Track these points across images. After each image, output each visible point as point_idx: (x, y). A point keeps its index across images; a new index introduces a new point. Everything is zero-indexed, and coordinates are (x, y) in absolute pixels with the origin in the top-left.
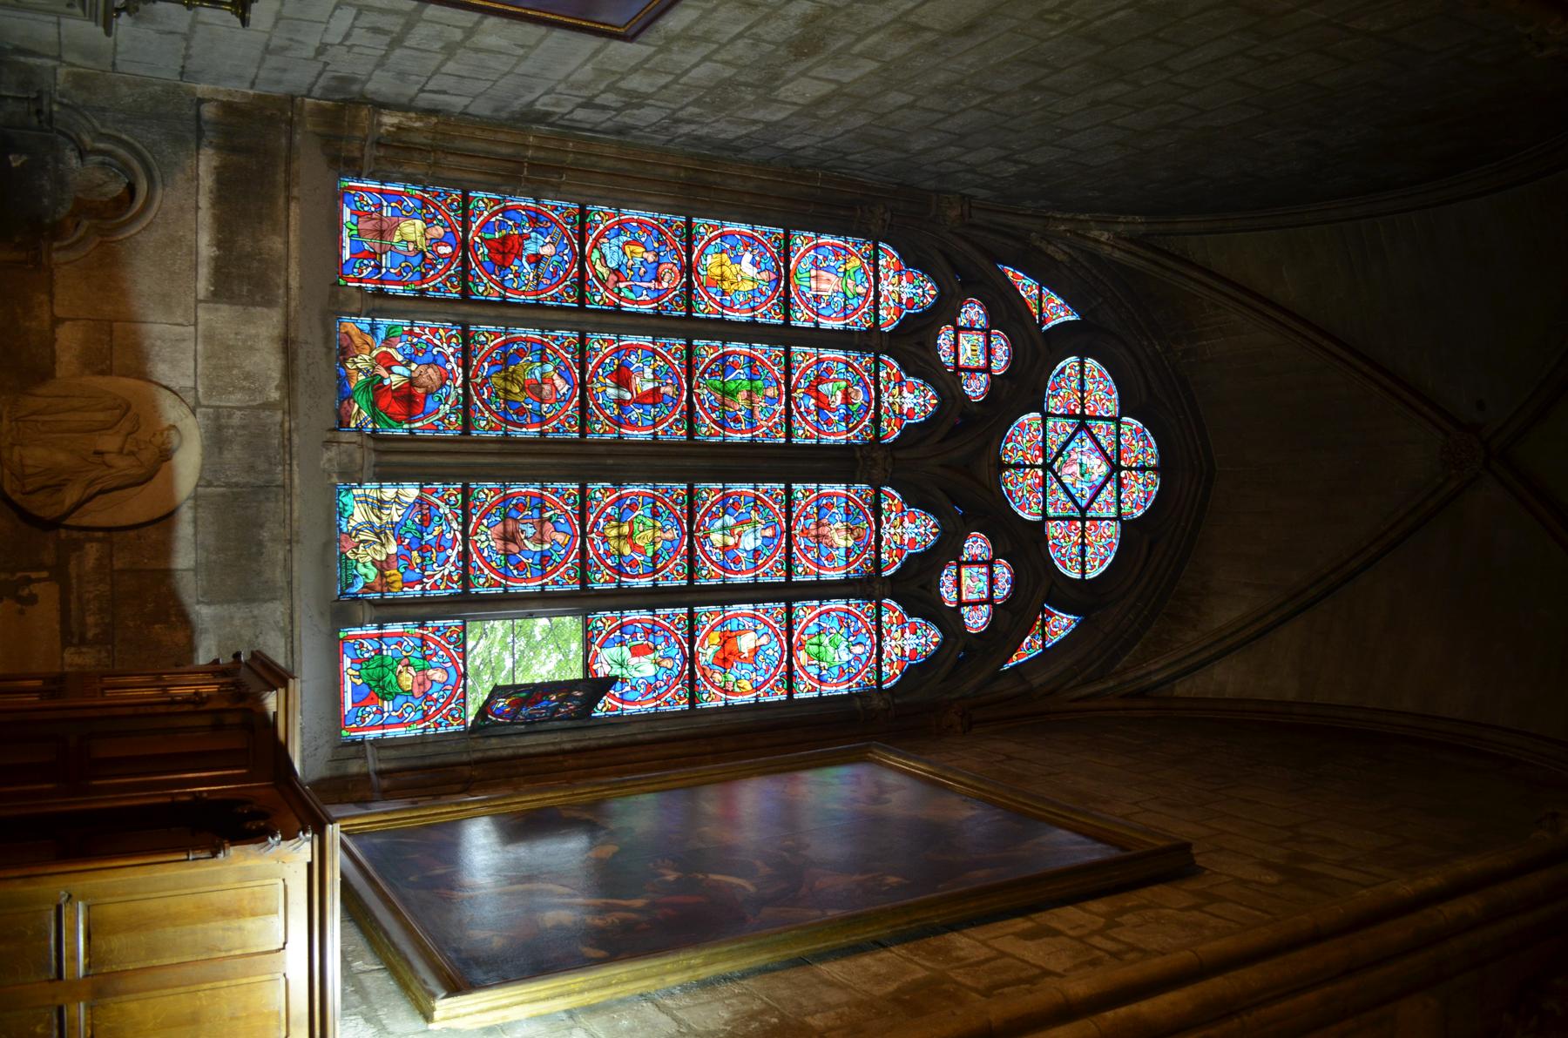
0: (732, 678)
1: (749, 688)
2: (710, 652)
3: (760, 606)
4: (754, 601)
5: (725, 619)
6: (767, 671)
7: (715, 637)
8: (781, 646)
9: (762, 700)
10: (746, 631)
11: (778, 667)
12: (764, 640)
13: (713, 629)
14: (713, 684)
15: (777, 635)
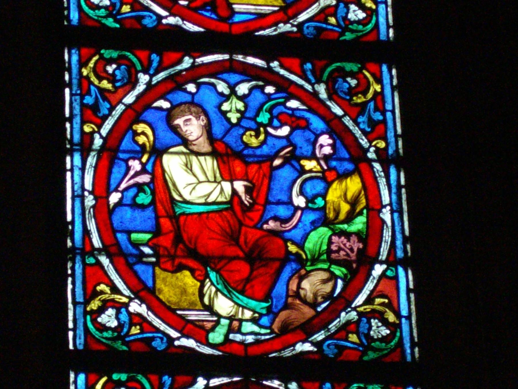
0: (318, 239)
1: (354, 185)
2: (224, 305)
3: (72, 130)
4: (55, 149)
5: (112, 249)
6: (297, 123)
7: (177, 286)
8: (216, 70)
9: (396, 145)
10: (160, 184)
11: (287, 89)
12: (193, 127)
13: (145, 292)
14: (343, 301)
15: (176, 83)
